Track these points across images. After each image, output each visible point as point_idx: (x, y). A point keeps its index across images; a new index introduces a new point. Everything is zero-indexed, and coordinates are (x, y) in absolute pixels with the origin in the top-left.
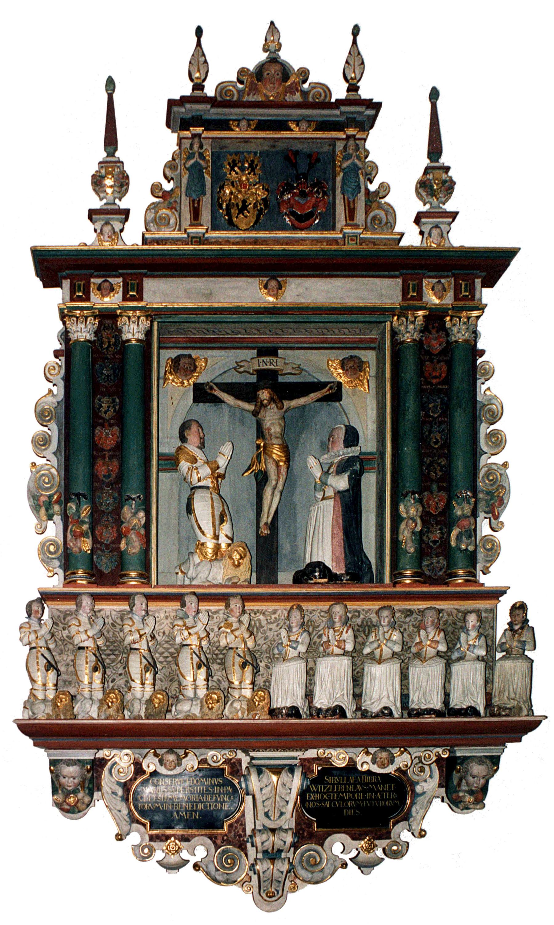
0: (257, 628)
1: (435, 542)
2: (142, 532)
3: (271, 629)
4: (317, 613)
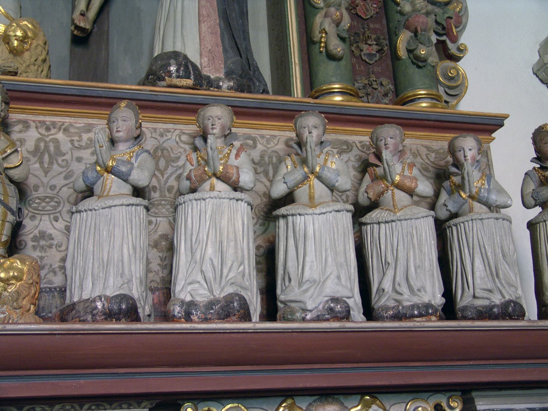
0: (50, 156)
1: (370, 55)
3: (79, 160)
4: (174, 136)
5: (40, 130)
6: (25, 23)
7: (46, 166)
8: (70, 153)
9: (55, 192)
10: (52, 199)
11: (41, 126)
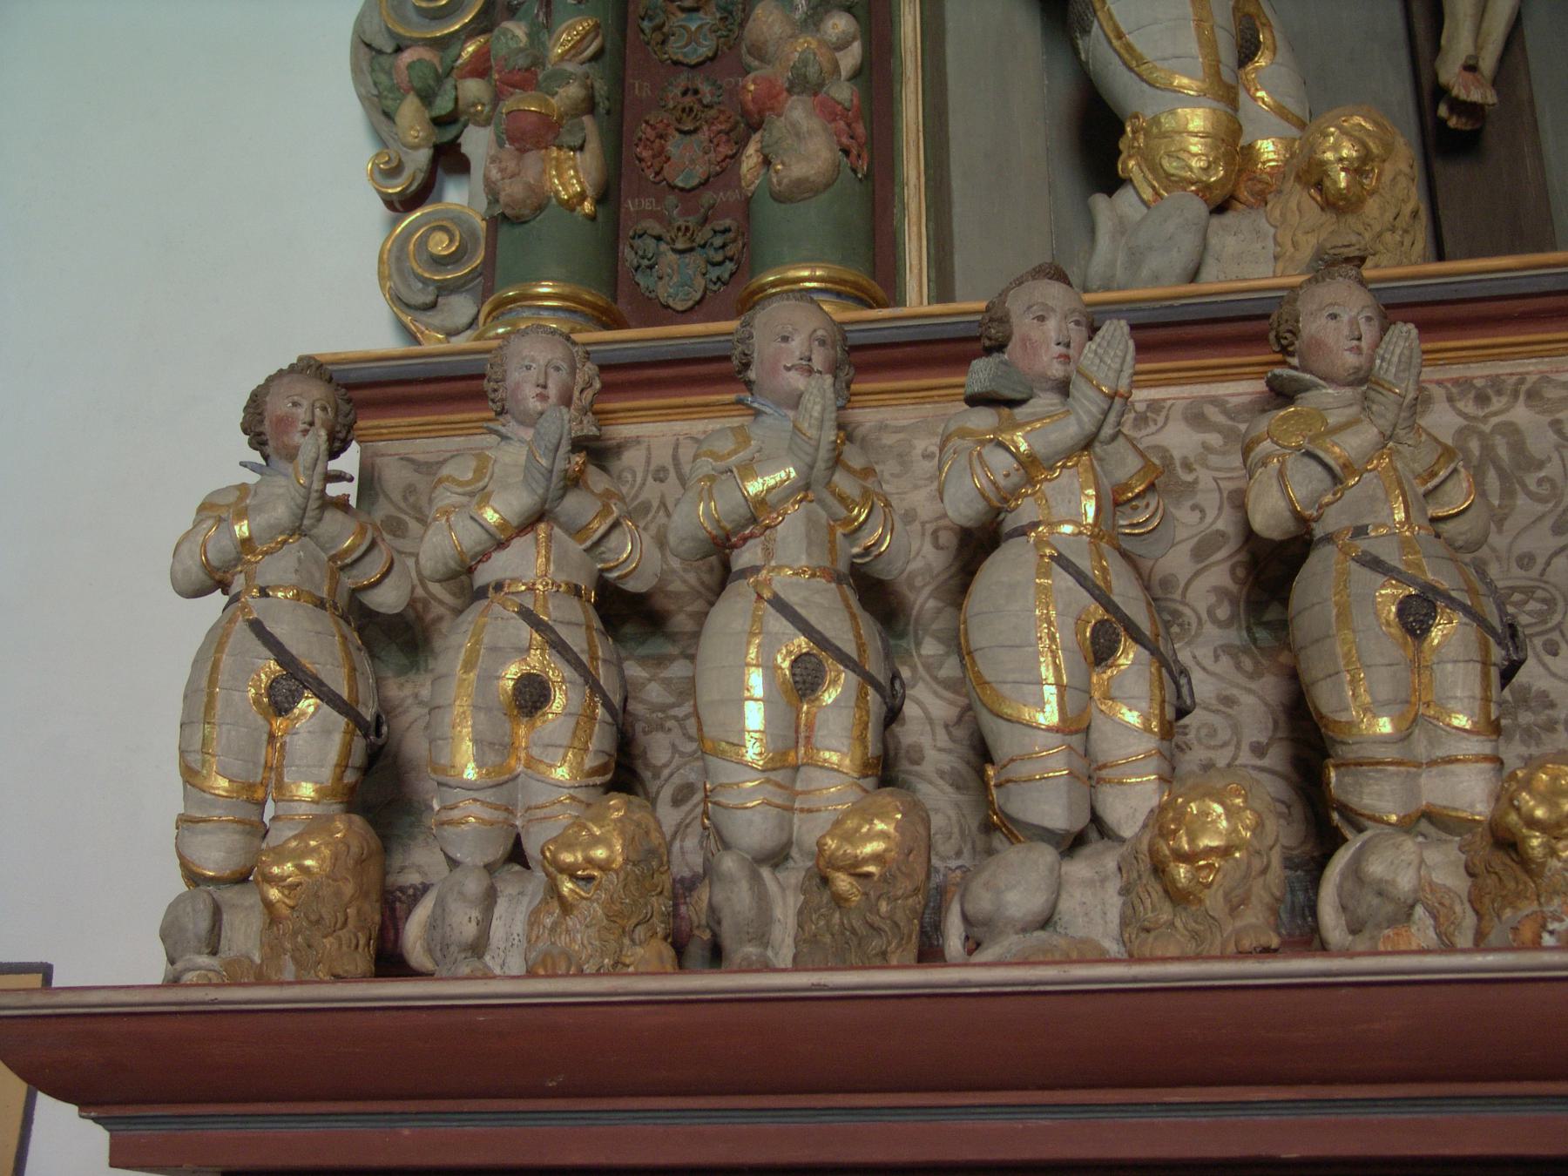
0: (1503, 476)
2: (843, 93)
5: (1460, 405)
6: (1358, 119)
7: (1496, 503)
8: (1555, 456)
9: (1535, 572)
10: (1529, 592)
11: (1463, 394)
